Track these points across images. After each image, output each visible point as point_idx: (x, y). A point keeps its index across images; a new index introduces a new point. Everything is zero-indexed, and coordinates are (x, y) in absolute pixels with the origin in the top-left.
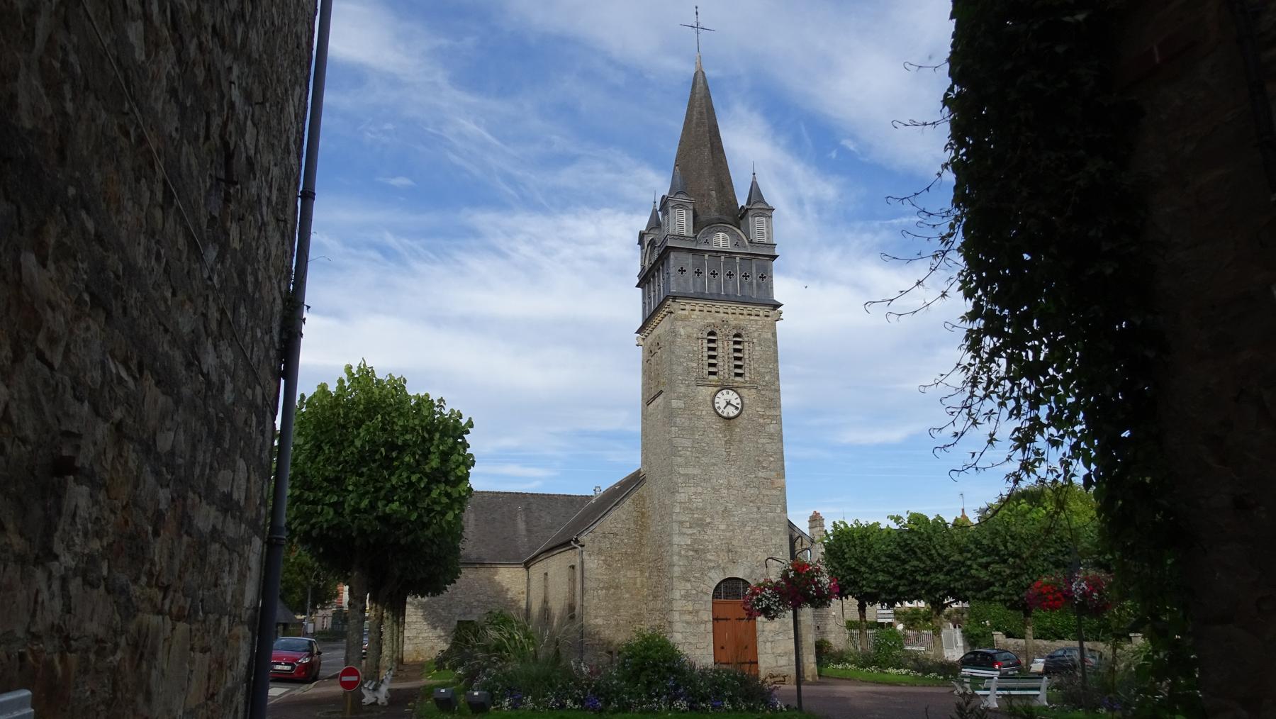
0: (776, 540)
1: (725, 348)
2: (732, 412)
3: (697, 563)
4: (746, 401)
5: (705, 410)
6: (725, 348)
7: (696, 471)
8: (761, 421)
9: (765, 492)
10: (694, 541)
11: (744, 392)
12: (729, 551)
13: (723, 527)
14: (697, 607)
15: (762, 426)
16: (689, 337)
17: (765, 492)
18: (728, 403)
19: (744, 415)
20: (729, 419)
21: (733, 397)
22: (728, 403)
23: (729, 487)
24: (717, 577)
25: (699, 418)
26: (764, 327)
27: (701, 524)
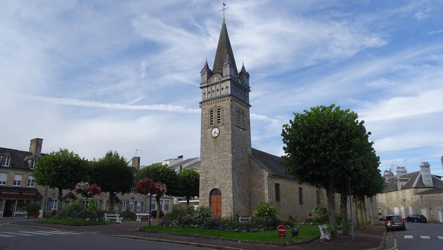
0: (228, 175)
1: (215, 114)
2: (216, 135)
3: (206, 185)
4: (221, 130)
5: (209, 136)
6: (215, 114)
7: (206, 156)
8: (225, 136)
9: (226, 159)
10: (205, 178)
11: (220, 128)
12: (214, 180)
13: (213, 172)
14: (205, 198)
15: (225, 137)
16: (206, 114)
17: (226, 159)
18: (215, 132)
19: (220, 135)
20: (216, 137)
21: (216, 130)
22: (215, 132)
23: (215, 159)
24: (211, 189)
25: (207, 139)
26: (227, 104)
27: (207, 172)
